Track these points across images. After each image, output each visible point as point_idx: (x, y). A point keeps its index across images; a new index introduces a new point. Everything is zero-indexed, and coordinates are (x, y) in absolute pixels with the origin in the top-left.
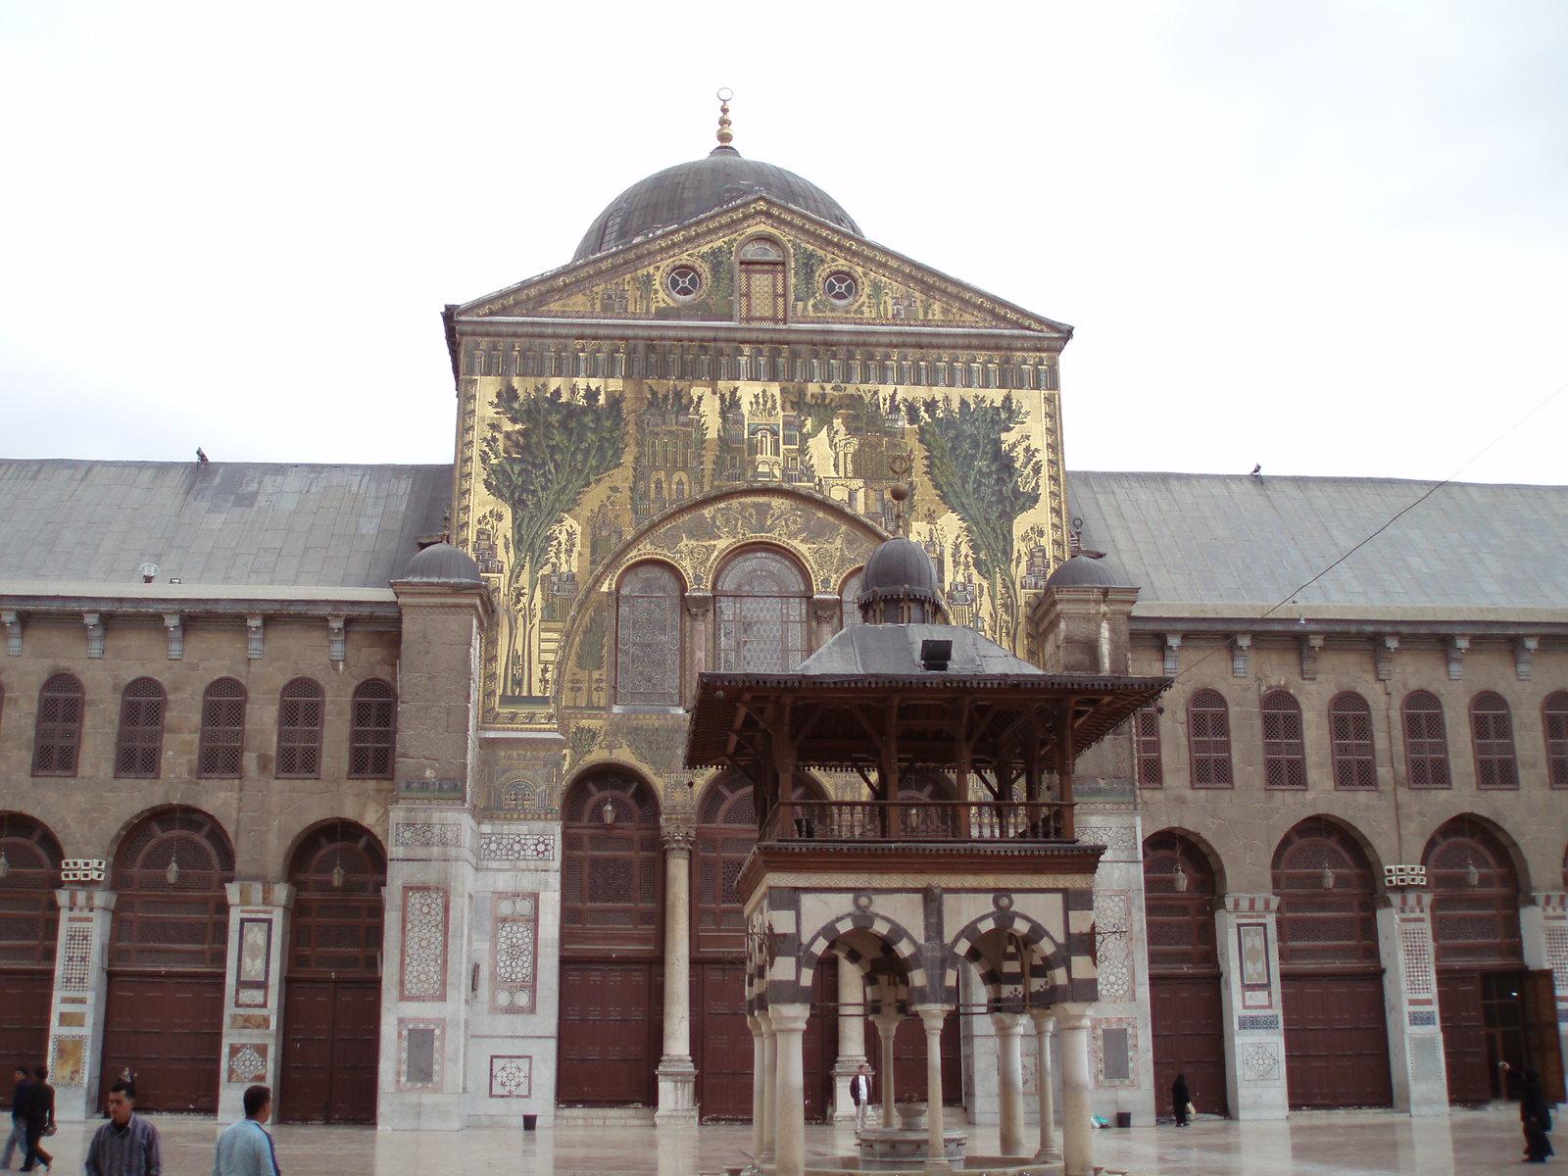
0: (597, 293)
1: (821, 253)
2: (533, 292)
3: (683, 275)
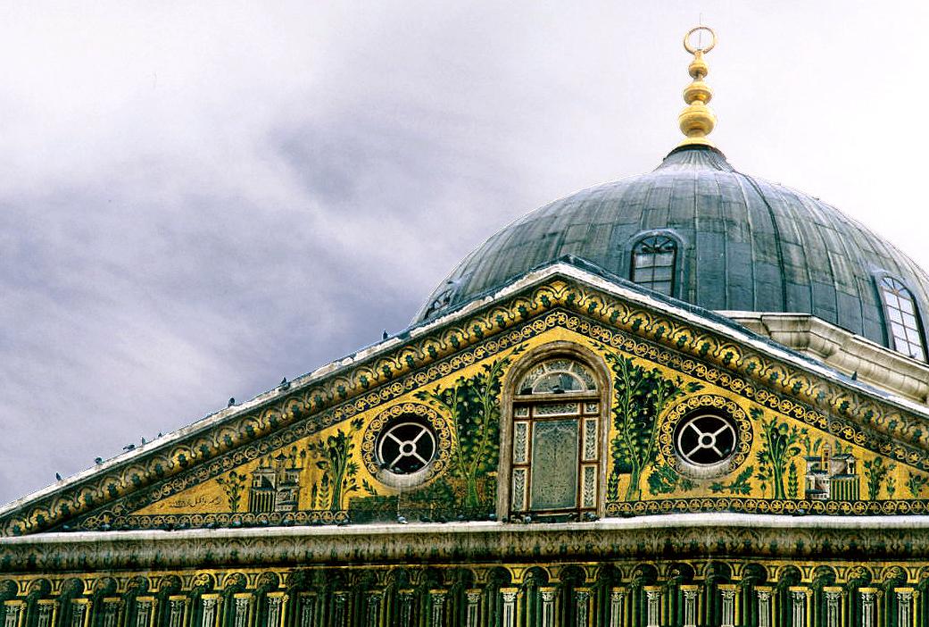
0: (243, 478)
1: (669, 374)
2: (124, 482)
3: (406, 434)
